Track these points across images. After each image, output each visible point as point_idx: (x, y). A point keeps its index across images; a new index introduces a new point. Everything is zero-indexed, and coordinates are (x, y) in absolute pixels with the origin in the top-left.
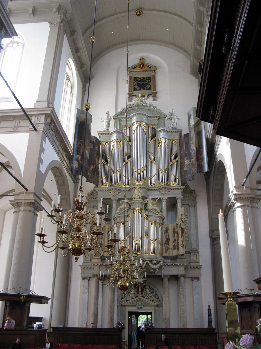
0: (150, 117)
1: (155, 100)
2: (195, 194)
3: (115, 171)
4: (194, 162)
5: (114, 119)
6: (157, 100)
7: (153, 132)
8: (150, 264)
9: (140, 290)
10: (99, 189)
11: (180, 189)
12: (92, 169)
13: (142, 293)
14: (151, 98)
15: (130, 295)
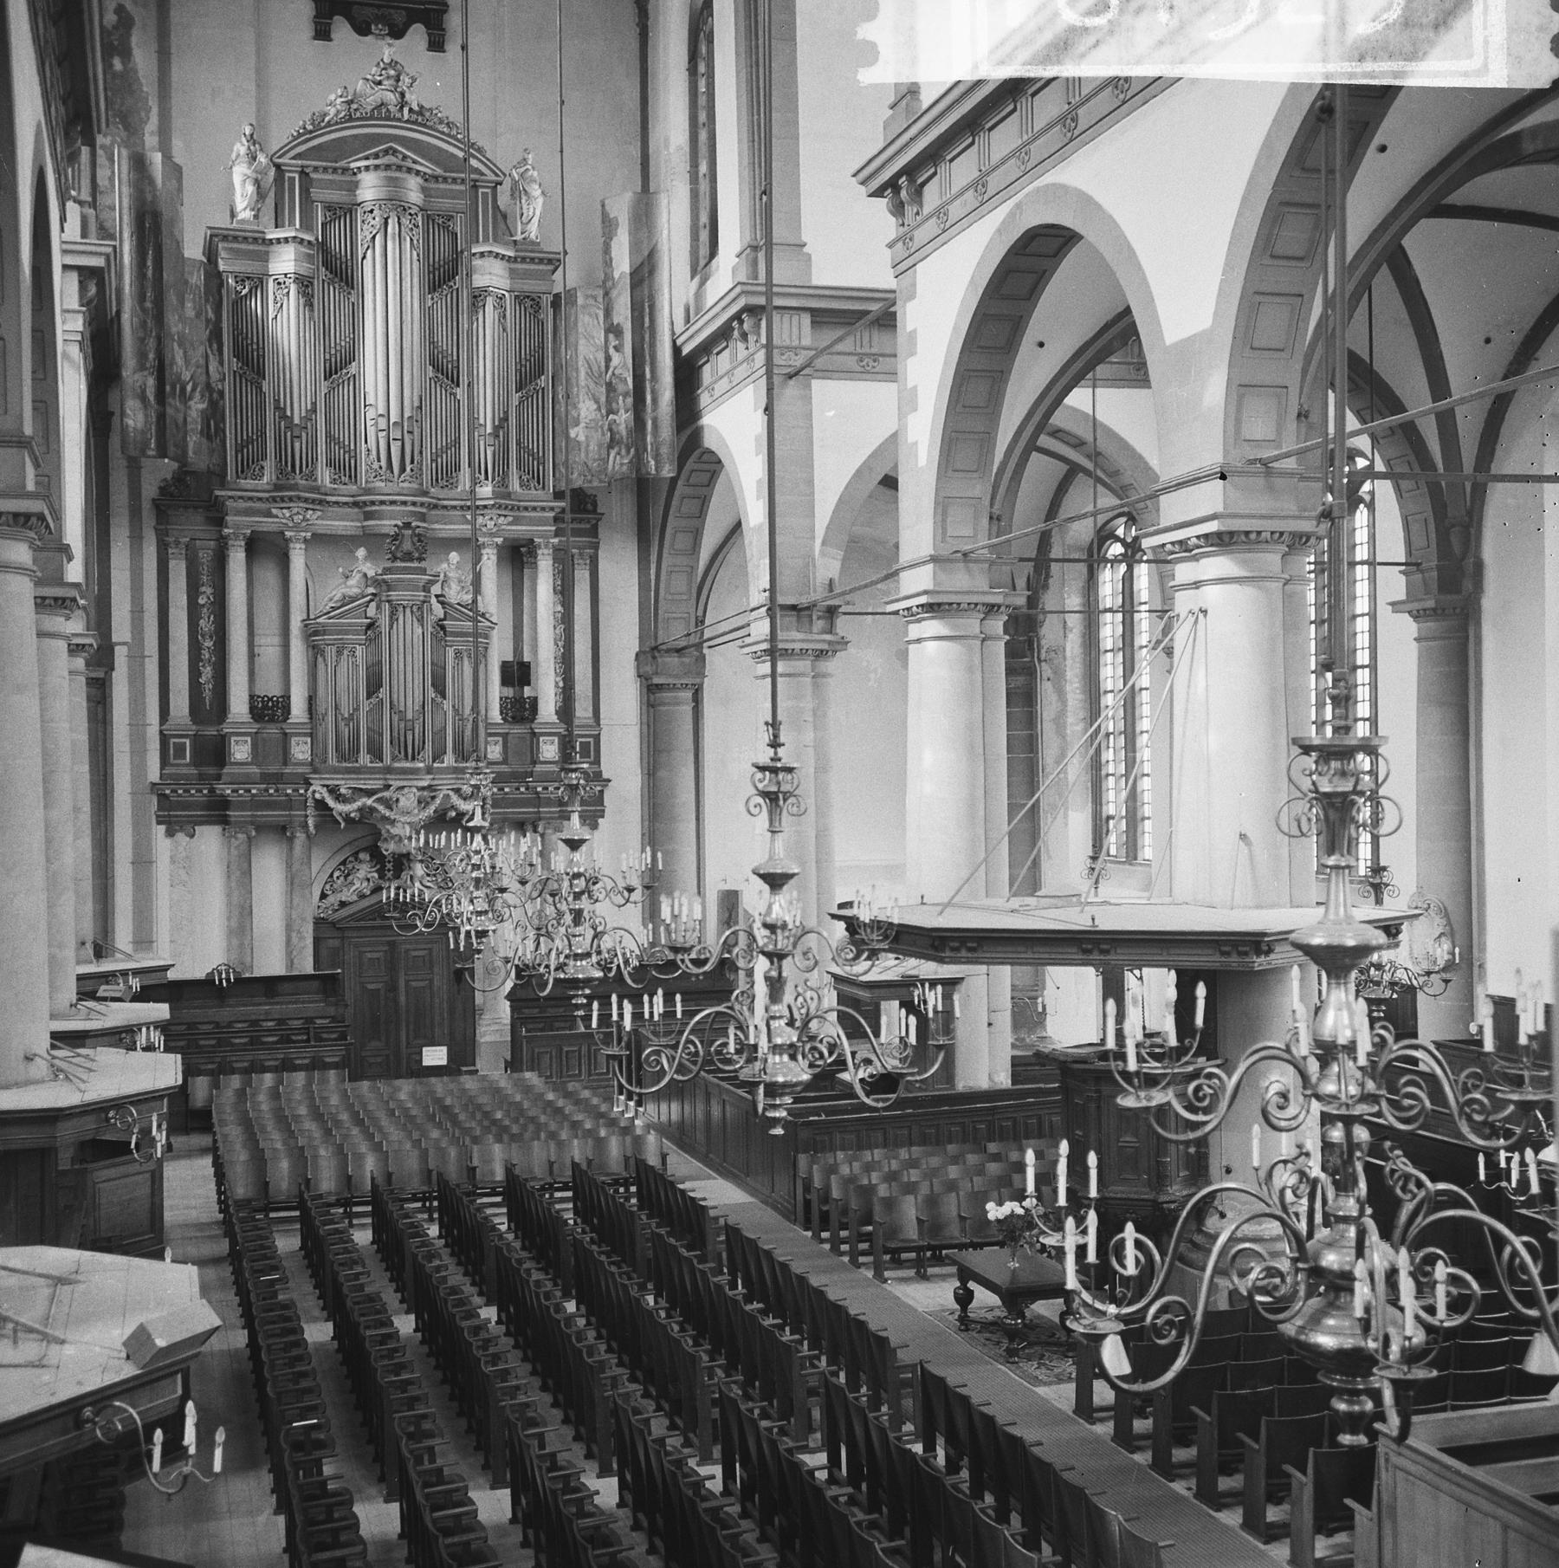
0: (436, 178)
1: (437, 45)
2: (594, 511)
3: (297, 421)
4: (622, 429)
5: (278, 167)
6: (446, 47)
7: (442, 249)
8: (455, 800)
9: (389, 866)
10: (230, 493)
11: (552, 509)
12: (203, 411)
13: (397, 876)
14: (417, 35)
15: (352, 883)
